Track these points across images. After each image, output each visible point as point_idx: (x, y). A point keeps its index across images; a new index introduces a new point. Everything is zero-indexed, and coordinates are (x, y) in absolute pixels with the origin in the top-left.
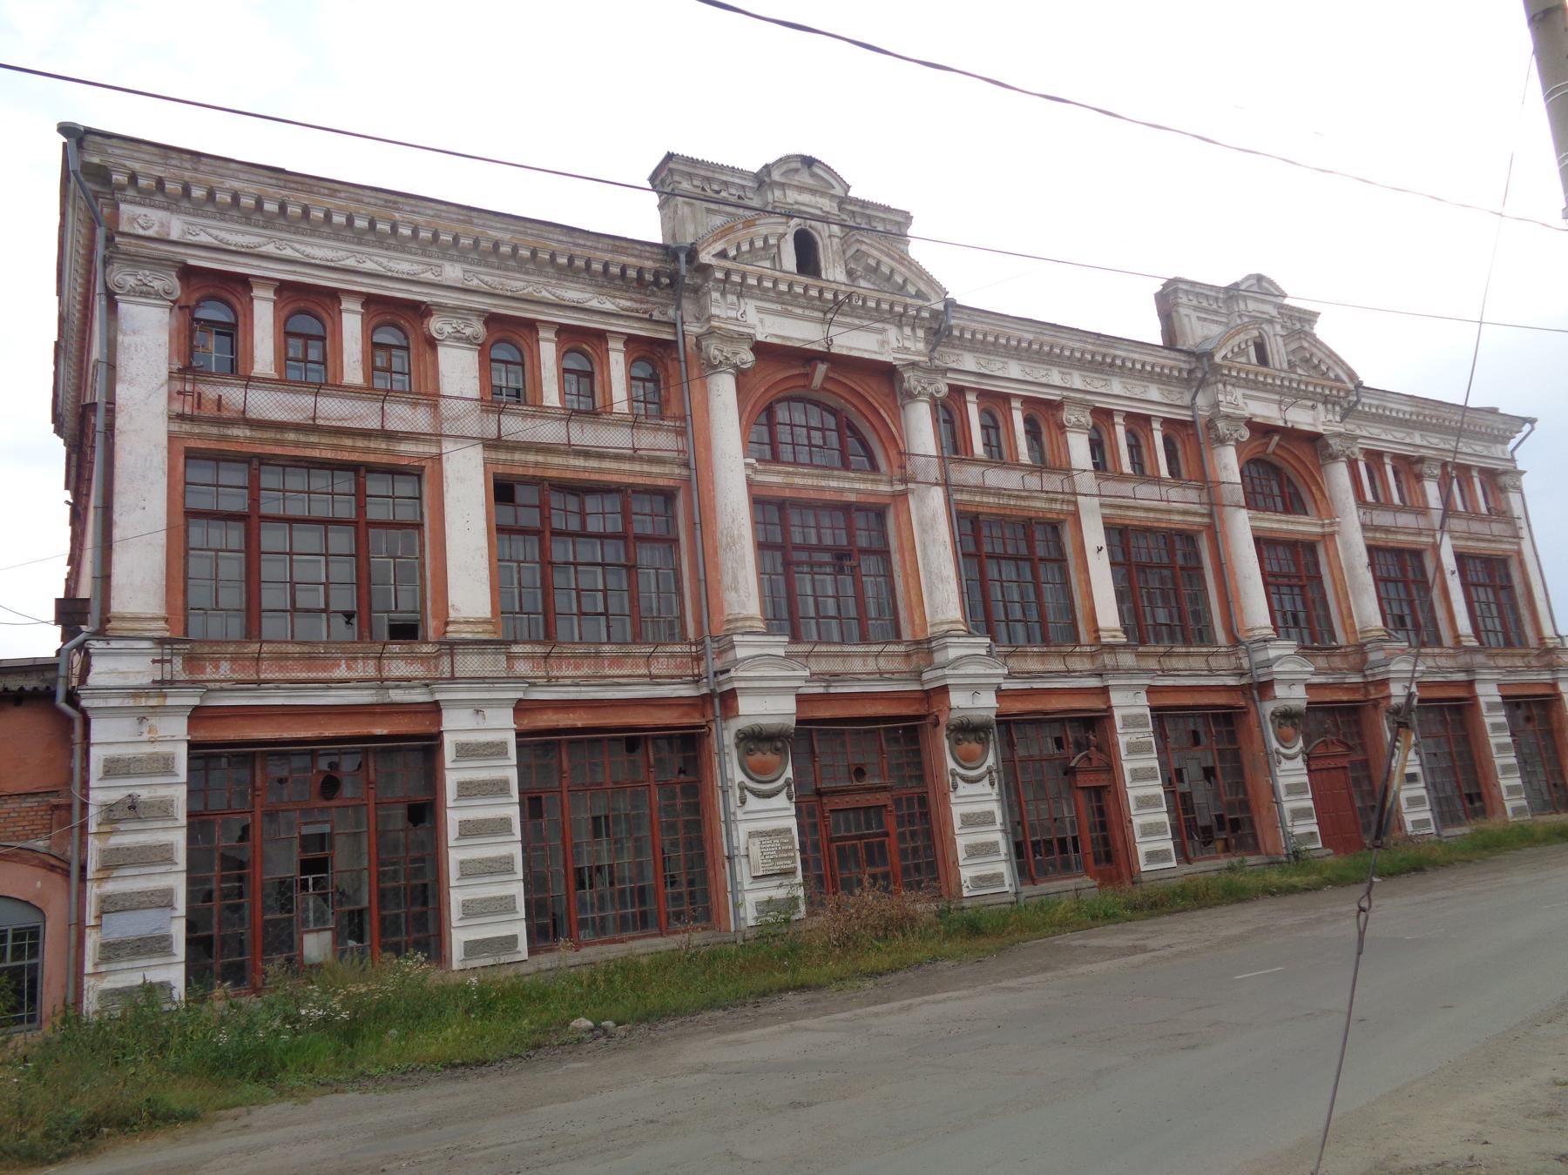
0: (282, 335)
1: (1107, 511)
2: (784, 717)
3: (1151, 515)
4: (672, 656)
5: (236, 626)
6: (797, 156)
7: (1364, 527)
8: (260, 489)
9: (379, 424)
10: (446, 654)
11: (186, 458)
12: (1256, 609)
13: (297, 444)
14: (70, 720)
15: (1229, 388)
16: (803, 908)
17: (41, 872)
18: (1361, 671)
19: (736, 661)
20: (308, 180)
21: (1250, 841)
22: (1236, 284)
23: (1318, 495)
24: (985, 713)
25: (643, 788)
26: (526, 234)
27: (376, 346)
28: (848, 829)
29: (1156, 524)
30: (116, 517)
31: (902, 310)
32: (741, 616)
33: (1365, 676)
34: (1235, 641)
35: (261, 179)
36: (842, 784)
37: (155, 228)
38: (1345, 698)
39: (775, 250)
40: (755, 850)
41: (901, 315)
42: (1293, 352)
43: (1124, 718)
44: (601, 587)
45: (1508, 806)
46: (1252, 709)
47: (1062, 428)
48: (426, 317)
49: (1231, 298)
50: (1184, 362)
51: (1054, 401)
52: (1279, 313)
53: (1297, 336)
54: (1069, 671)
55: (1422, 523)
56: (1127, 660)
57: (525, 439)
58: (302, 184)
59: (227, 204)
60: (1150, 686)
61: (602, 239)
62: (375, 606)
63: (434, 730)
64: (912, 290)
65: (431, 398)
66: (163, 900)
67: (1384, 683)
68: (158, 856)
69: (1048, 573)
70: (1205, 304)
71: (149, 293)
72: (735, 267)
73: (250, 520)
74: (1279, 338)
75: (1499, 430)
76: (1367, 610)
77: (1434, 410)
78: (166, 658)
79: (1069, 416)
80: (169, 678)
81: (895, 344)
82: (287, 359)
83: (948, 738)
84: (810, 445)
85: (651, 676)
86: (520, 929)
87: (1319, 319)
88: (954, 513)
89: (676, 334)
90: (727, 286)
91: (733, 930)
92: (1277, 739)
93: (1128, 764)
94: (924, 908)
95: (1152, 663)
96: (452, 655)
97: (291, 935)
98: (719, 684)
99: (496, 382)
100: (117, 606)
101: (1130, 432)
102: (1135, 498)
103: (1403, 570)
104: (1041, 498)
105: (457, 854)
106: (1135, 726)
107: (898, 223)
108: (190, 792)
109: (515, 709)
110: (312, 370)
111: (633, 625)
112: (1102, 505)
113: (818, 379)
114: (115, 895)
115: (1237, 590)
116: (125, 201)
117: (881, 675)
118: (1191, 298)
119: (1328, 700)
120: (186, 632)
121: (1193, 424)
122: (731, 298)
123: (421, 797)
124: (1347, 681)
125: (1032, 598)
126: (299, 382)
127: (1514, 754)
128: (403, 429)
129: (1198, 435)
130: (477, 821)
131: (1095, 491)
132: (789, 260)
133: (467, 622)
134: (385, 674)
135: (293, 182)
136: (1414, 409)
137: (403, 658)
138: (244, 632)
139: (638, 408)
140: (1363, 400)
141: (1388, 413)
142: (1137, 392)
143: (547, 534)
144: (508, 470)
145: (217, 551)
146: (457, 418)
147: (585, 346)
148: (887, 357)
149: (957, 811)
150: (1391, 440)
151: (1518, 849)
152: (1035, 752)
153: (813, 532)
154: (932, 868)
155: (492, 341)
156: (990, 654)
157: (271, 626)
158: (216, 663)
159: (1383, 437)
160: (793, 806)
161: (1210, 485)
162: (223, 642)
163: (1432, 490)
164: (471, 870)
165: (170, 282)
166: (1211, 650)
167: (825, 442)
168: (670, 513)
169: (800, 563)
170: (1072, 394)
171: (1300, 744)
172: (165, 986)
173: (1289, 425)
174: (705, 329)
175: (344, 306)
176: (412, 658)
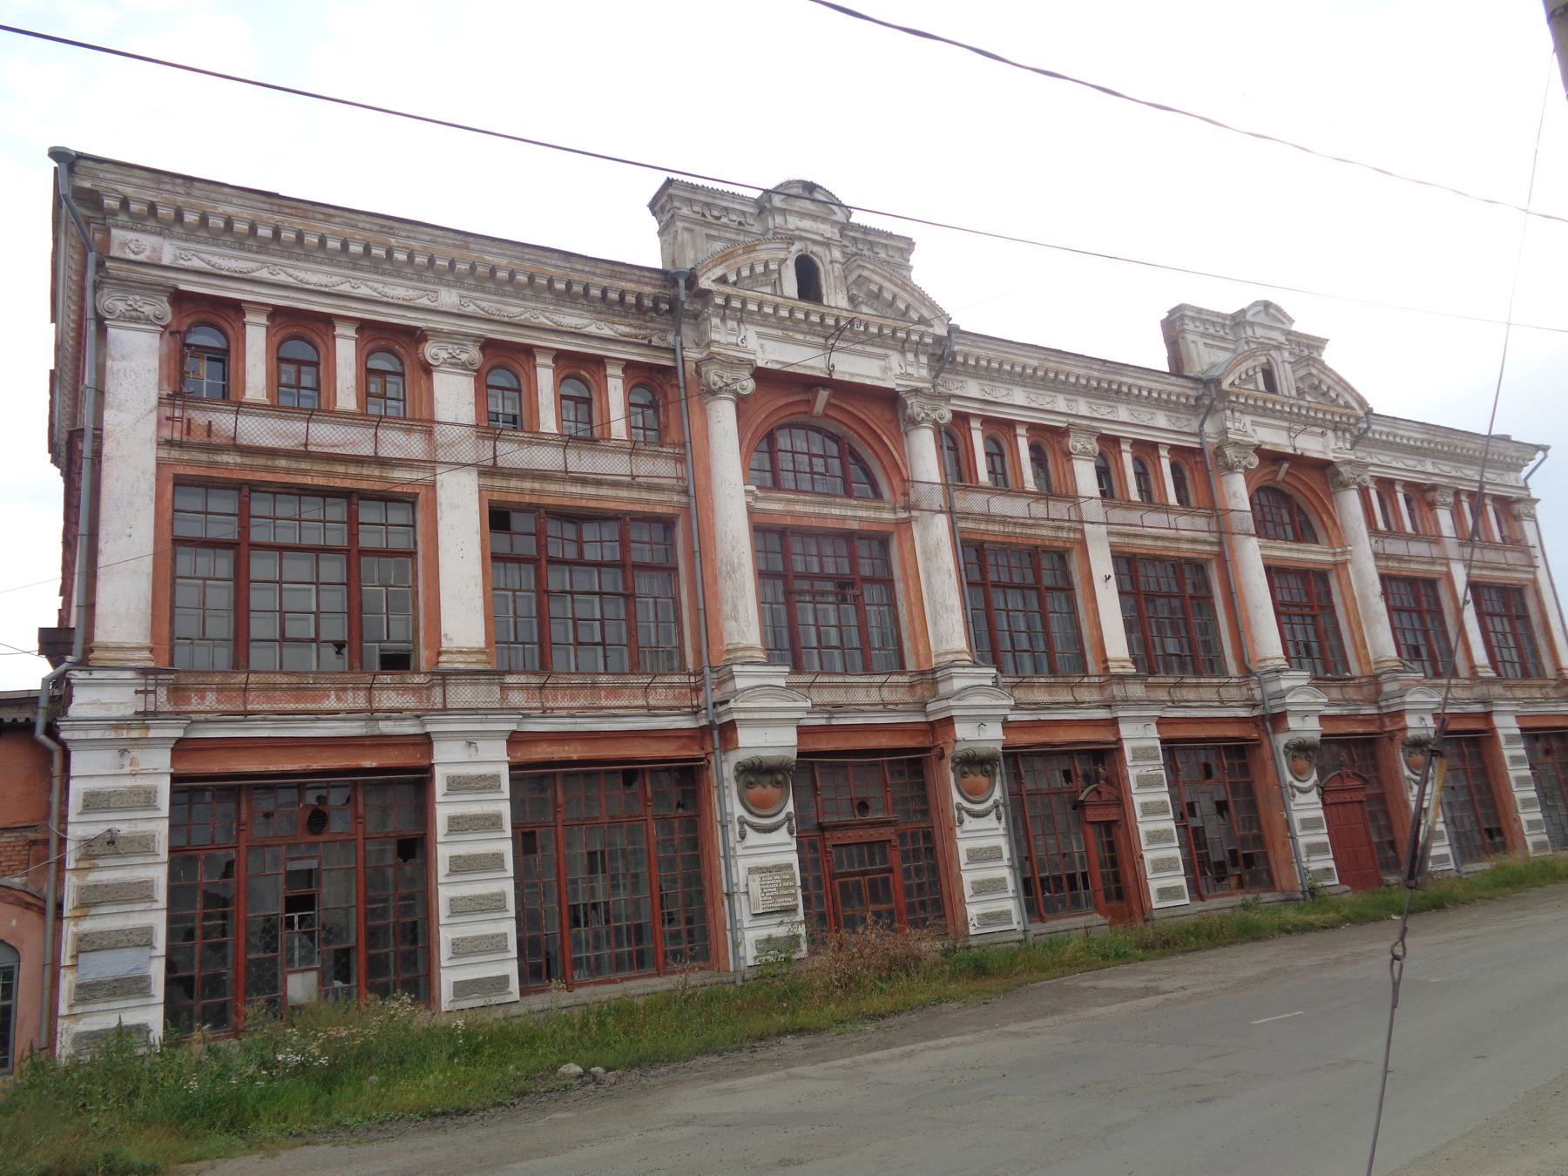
0: (275, 360)
1: (1115, 539)
2: (784, 749)
3: (1160, 543)
4: (671, 686)
5: (223, 656)
6: (798, 182)
7: (1377, 556)
8: (251, 517)
9: (372, 450)
10: (439, 685)
11: (175, 485)
12: (1268, 640)
13: (288, 471)
14: (49, 753)
15: (1237, 414)
16: (804, 946)
17: (17, 910)
18: (1375, 702)
19: (736, 692)
20: (301, 205)
21: (1265, 876)
22: (1243, 312)
23: (1329, 524)
24: (991, 745)
25: (640, 823)
26: (523, 259)
27: (370, 372)
28: (851, 865)
29: (1164, 553)
30: (101, 545)
31: (904, 336)
32: (741, 646)
33: (1380, 708)
34: (1246, 672)
35: (255, 204)
36: (845, 818)
37: (147, 253)
38: (1360, 730)
39: (776, 276)
40: (755, 887)
41: (905, 341)
42: (1302, 379)
43: (1134, 750)
44: (598, 616)
45: (1529, 841)
46: (1266, 742)
47: (1068, 455)
48: (421, 342)
49: (1238, 324)
50: (1192, 389)
51: (1060, 428)
52: (1287, 340)
53: (1306, 363)
54: (1076, 703)
55: (1435, 551)
56: (1136, 690)
57: (521, 466)
58: (296, 208)
59: (219, 229)
60: (1160, 718)
61: (600, 265)
62: (366, 636)
63: (425, 762)
64: (915, 316)
65: (426, 424)
66: (142, 939)
67: (1400, 714)
68: (139, 893)
69: (1055, 602)
70: (1212, 331)
71: (140, 319)
72: (735, 293)
73: (240, 549)
74: (1287, 365)
75: (1512, 458)
76: (1381, 640)
78: (149, 688)
79: (1075, 443)
80: (152, 708)
81: (898, 371)
82: (280, 385)
83: (953, 771)
84: (812, 472)
85: (649, 708)
86: (511, 969)
87: (1327, 346)
88: (958, 540)
89: (675, 360)
90: (727, 311)
91: (732, 969)
92: (1291, 772)
93: (1139, 798)
94: (929, 947)
95: (1162, 695)
96: (444, 686)
97: (275, 975)
98: (719, 715)
99: (492, 408)
100: (100, 636)
101: (1137, 460)
102: (1143, 526)
103: (1417, 600)
104: (1048, 527)
105: (447, 891)
106: (1146, 759)
107: (900, 250)
108: (171, 826)
109: (509, 742)
110: (306, 397)
111: (631, 656)
112: (1109, 533)
113: (819, 406)
114: (93, 934)
115: (1248, 619)
116: (117, 226)
117: (885, 706)
118: (1197, 324)
120: (172, 663)
121: (1201, 451)
122: (731, 324)
123: (409, 831)
124: (1362, 712)
125: (1039, 627)
126: (289, 407)
127: (1533, 788)
128: (397, 456)
129: (1206, 464)
130: (469, 856)
131: (1102, 519)
132: (791, 286)
133: (461, 652)
134: (376, 705)
135: (286, 207)
137: (394, 689)
138: (231, 664)
139: (637, 435)
140: (1374, 427)
141: (1398, 440)
142: (1145, 418)
143: (544, 562)
144: (503, 497)
145: (205, 579)
146: (452, 445)
147: (583, 373)
148: (890, 384)
149: (963, 847)
150: (1403, 468)
151: (1541, 886)
152: (1043, 785)
153: (815, 560)
154: (938, 904)
155: (488, 366)
156: (996, 684)
157: (260, 656)
158: (202, 693)
159: (1394, 464)
160: (794, 841)
161: (1219, 512)
162: (208, 672)
163: (1444, 518)
164: (461, 907)
165: (161, 307)
166: (1222, 680)
167: (827, 470)
168: (669, 542)
169: (802, 592)
170: (1078, 421)
171: (1315, 777)
172: (142, 1029)
173: (1299, 452)
174: (704, 354)
175: (339, 331)
176: (405, 689)
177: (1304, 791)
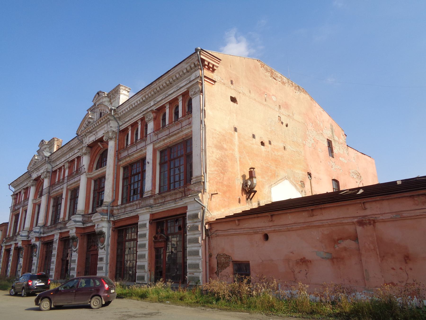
29: (77, 186)
107: (53, 141)
136: (142, 96)
171: (78, 247)
177: (75, 251)
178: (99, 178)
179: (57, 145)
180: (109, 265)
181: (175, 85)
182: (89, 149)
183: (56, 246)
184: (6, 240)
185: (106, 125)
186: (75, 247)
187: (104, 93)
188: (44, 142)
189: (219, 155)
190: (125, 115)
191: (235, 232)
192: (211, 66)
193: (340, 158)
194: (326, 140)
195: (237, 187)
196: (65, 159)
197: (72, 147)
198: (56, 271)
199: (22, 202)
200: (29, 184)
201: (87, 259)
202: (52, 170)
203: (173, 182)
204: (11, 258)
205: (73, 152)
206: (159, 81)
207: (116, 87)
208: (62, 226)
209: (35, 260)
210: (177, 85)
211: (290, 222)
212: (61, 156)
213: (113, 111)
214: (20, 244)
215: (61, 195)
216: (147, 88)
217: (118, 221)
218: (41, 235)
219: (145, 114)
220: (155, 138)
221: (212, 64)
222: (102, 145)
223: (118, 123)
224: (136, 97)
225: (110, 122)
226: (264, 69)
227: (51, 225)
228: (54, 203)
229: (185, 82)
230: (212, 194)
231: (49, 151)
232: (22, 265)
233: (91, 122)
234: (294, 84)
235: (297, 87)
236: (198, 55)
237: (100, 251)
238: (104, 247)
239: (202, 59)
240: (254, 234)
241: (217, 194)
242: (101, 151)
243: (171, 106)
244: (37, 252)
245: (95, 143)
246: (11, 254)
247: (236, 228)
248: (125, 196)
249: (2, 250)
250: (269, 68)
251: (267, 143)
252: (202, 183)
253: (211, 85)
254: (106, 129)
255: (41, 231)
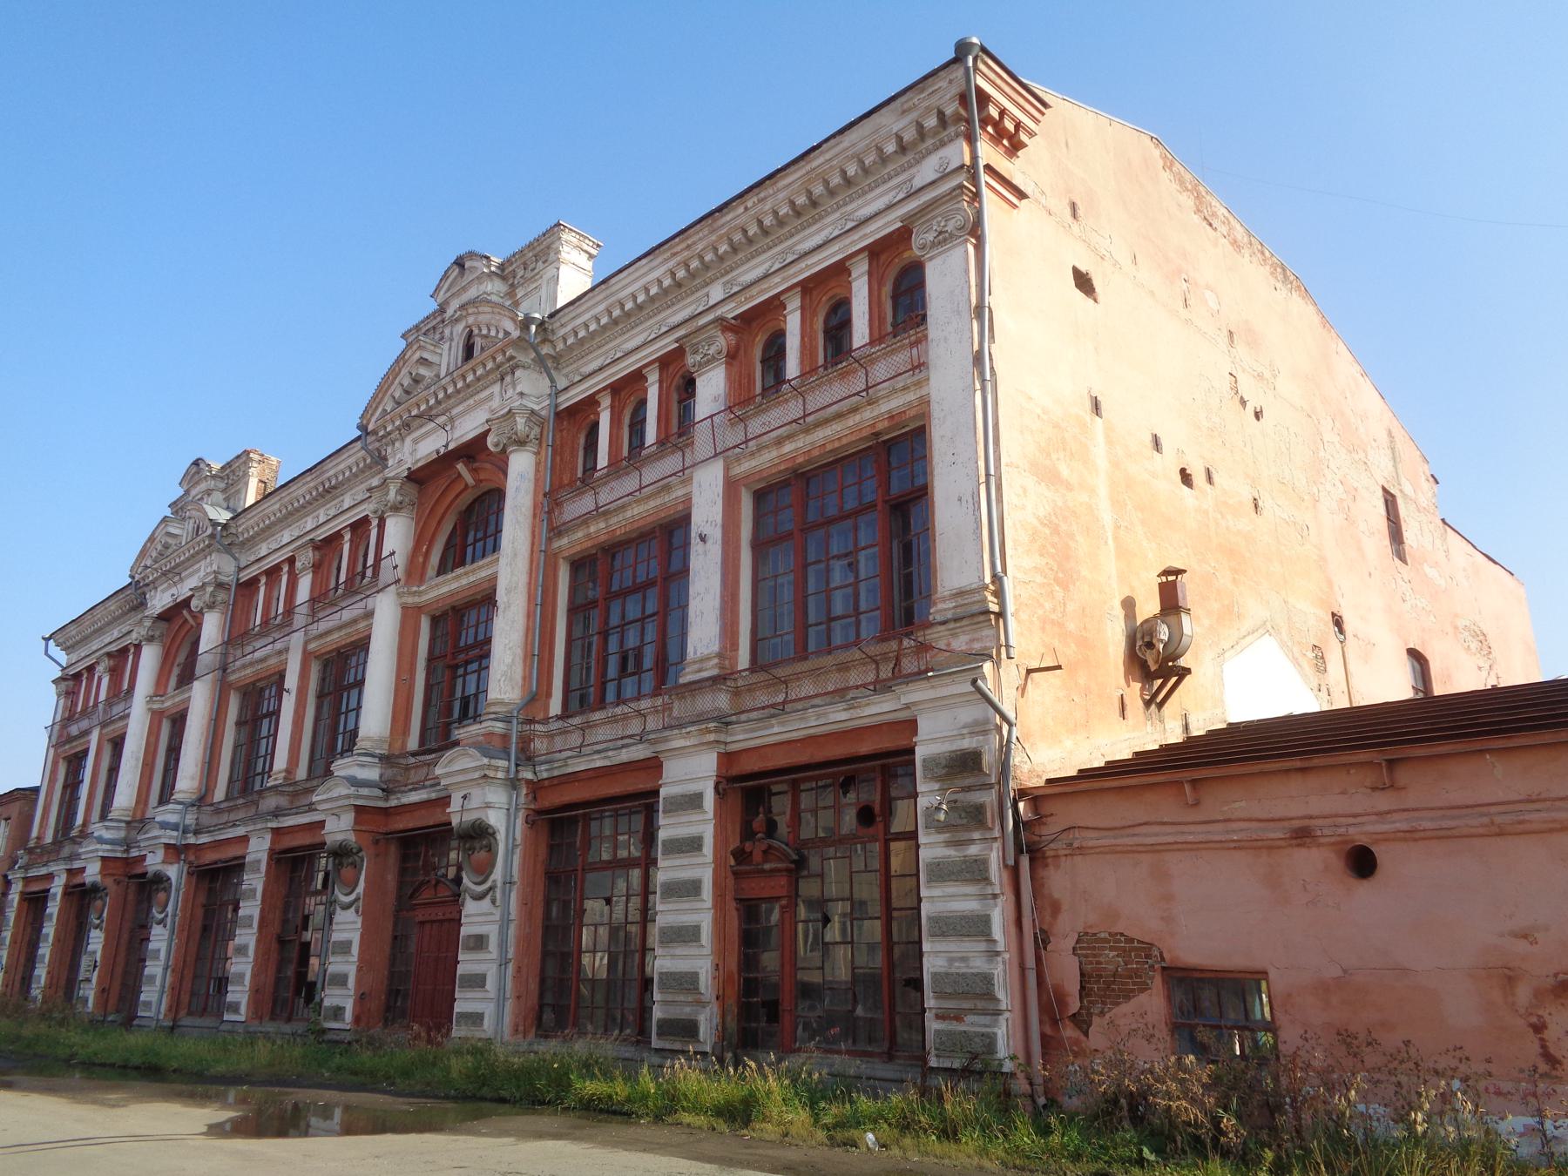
3: (343, 632)
29: (348, 641)
77: (711, 232)
107: (245, 463)
115: (208, 732)
119: (431, 823)
177: (346, 907)
178: (453, 608)
179: (261, 481)
180: (511, 966)
181: (835, 211)
182: (412, 489)
183: (254, 882)
184: (26, 858)
185: (496, 388)
186: (349, 890)
187: (487, 258)
188: (202, 466)
189: (1047, 507)
190: (583, 345)
191: (1180, 839)
192: (1010, 126)
193: (1427, 569)
194: (1380, 492)
195: (1111, 649)
196: (296, 534)
197: (333, 482)
198: (256, 991)
199: (101, 706)
200: (134, 635)
201: (398, 940)
202: (238, 580)
203: (824, 619)
204: (49, 929)
205: (333, 503)
206: (762, 195)
207: (544, 235)
208: (283, 801)
209: (160, 939)
210: (843, 210)
211: (1501, 796)
212: (280, 520)
213: (533, 328)
214: (93, 873)
215: (277, 677)
216: (698, 226)
217: (555, 782)
218: (186, 838)
219: (686, 336)
220: (733, 437)
221: (1013, 119)
222: (474, 471)
223: (552, 380)
224: (646, 269)
225: (518, 373)
226: (1172, 178)
227: (227, 799)
228: (241, 709)
229: (881, 195)
230: (1029, 671)
231: (225, 505)
232: (98, 959)
233: (424, 377)
234: (1267, 254)
235: (1279, 270)
236: (967, 69)
237: (470, 907)
238: (491, 889)
239: (979, 90)
240: (1291, 845)
241: (1059, 667)
242: (467, 498)
243: (811, 299)
244: (170, 909)
245: (445, 461)
246: (51, 915)
247: (1180, 820)
248: (575, 684)
249: (10, 897)
250: (1188, 177)
251: (1199, 478)
252: (992, 616)
253: (1006, 206)
254: (495, 403)
255: (188, 822)
